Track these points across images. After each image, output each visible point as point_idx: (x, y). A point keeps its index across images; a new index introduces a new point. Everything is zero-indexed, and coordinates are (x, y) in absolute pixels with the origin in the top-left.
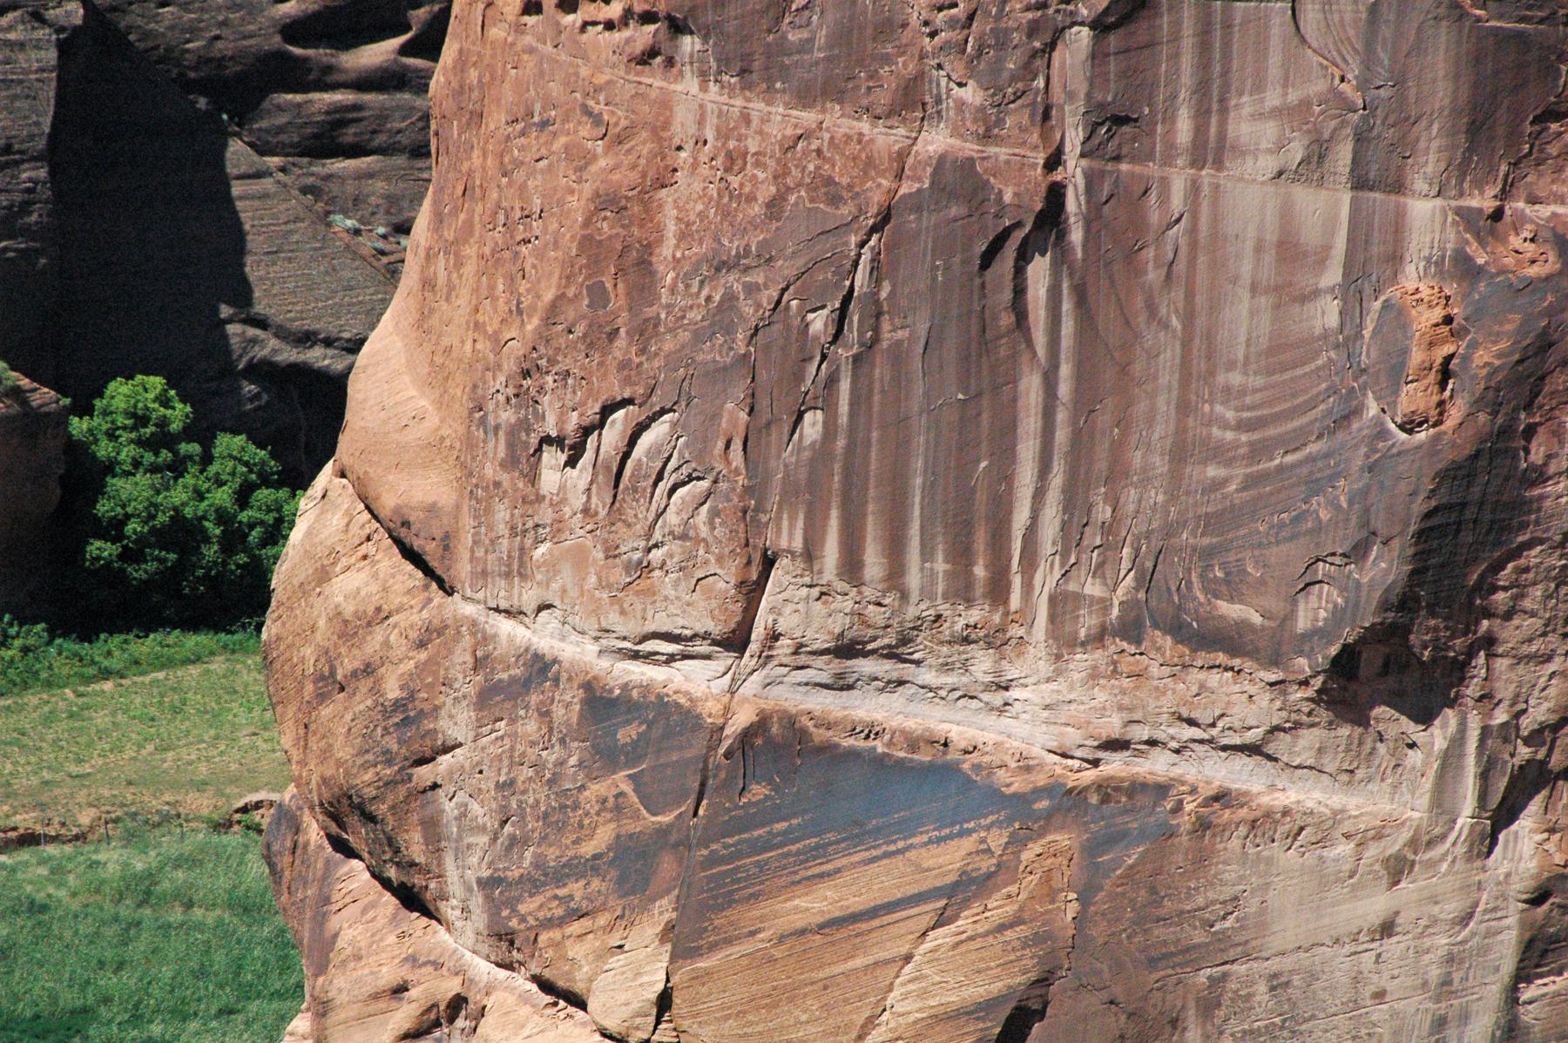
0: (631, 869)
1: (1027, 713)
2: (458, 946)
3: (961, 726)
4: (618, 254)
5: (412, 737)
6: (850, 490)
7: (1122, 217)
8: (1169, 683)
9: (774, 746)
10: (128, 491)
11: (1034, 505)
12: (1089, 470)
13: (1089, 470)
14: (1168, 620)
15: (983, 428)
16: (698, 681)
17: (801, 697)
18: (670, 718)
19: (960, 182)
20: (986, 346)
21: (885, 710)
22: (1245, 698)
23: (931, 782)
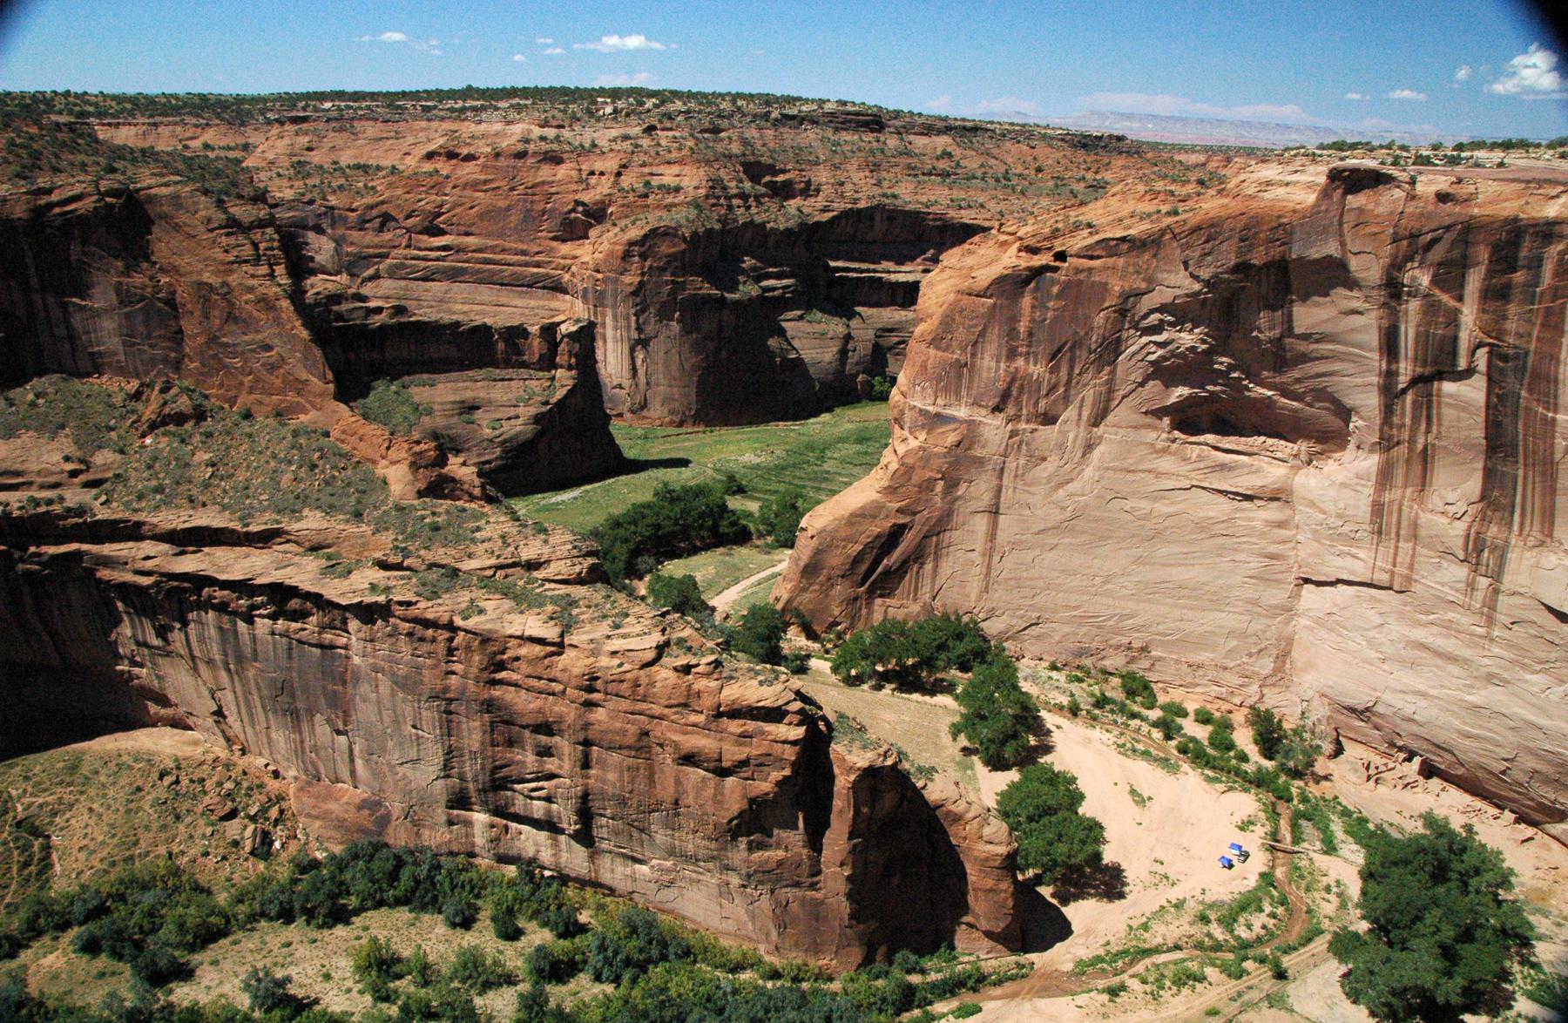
0: (923, 427)
1: (962, 412)
2: (906, 433)
3: (956, 414)
4: (924, 366)
5: (902, 412)
6: (946, 390)
7: (973, 365)
8: (976, 409)
9: (938, 415)
10: (878, 388)
11: (964, 393)
12: (969, 388)
13: (969, 388)
14: (976, 403)
15: (959, 385)
16: (930, 408)
17: (940, 410)
18: (927, 412)
19: (957, 360)
20: (960, 376)
21: (948, 412)
22: (984, 412)
23: (953, 419)
